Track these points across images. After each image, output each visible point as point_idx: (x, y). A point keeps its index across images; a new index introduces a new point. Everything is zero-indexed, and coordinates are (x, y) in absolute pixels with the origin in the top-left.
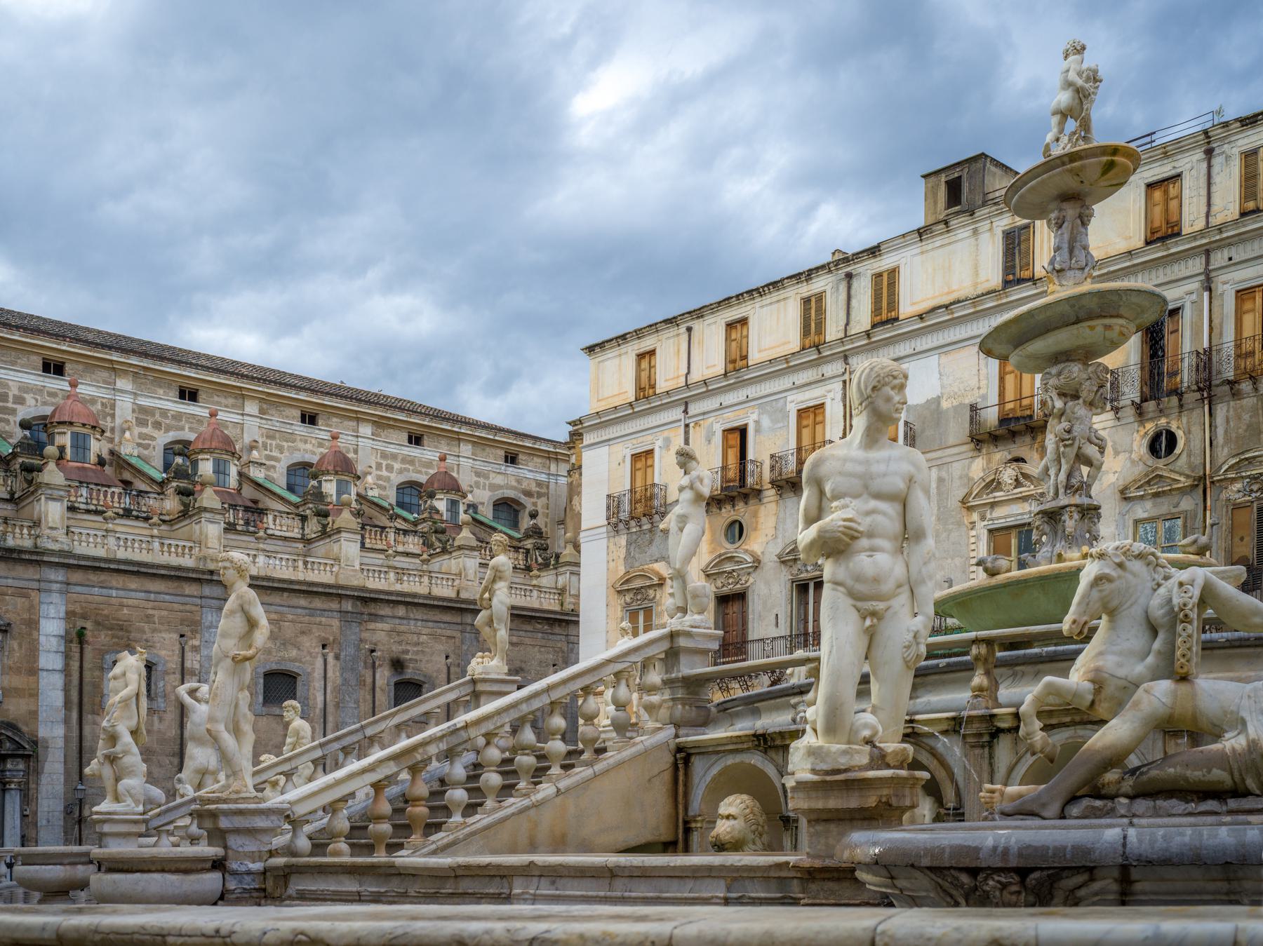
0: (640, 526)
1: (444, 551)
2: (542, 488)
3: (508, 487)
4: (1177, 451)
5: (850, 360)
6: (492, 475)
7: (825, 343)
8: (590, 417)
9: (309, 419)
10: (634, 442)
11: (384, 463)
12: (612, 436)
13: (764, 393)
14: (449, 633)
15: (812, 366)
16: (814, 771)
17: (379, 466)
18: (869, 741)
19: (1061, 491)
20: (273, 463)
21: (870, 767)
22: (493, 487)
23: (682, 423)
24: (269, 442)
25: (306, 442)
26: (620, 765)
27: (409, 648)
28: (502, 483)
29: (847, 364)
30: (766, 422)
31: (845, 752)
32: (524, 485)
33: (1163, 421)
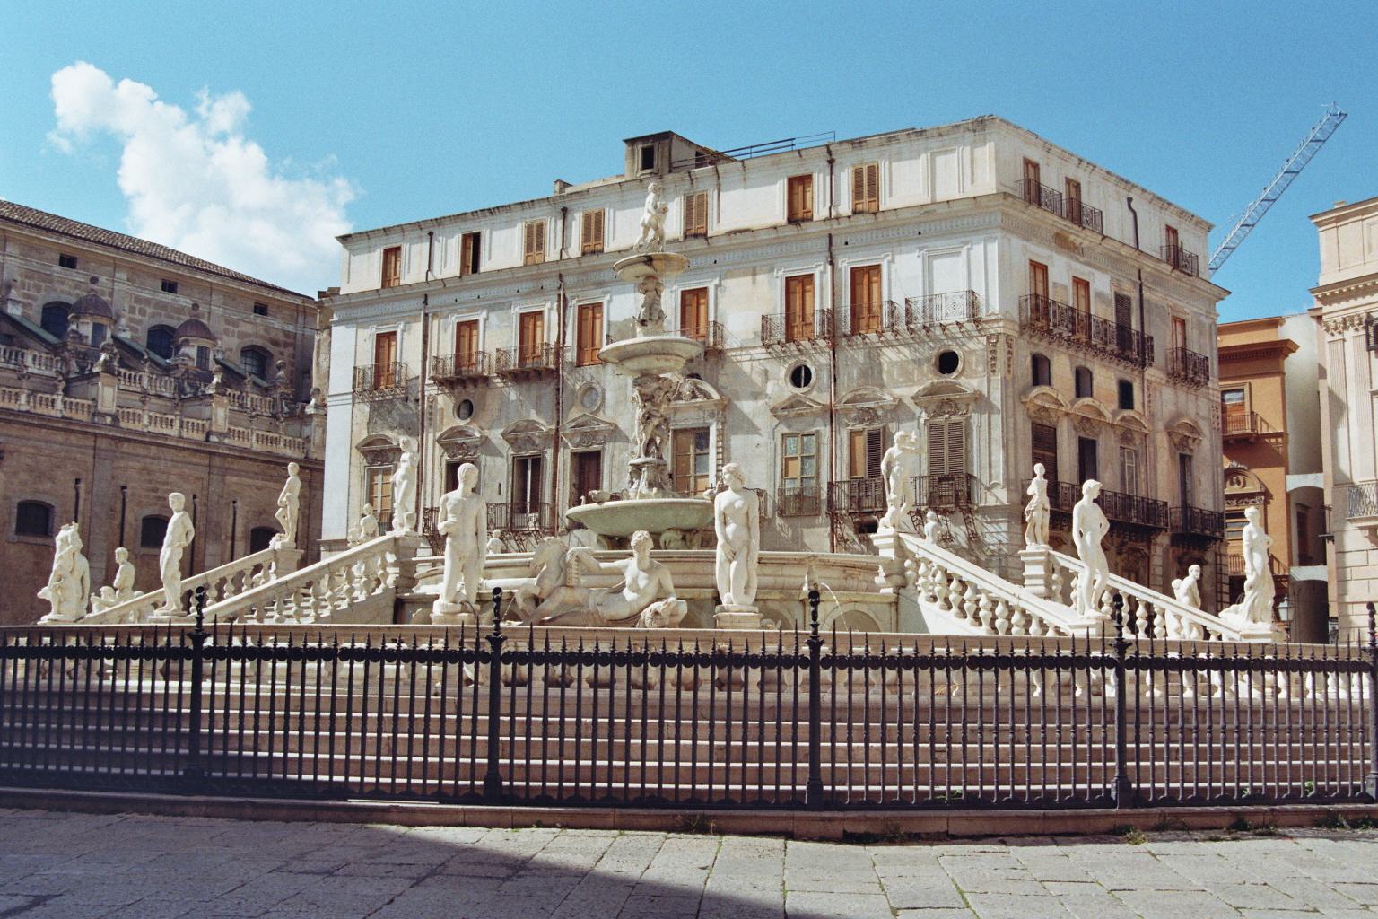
1: (195, 397)
3: (256, 336)
9: (68, 262)
11: (137, 306)
14: (197, 474)
17: (132, 310)
20: (29, 301)
22: (242, 335)
24: (27, 281)
25: (63, 283)
27: (158, 486)
28: (251, 332)
32: (273, 335)
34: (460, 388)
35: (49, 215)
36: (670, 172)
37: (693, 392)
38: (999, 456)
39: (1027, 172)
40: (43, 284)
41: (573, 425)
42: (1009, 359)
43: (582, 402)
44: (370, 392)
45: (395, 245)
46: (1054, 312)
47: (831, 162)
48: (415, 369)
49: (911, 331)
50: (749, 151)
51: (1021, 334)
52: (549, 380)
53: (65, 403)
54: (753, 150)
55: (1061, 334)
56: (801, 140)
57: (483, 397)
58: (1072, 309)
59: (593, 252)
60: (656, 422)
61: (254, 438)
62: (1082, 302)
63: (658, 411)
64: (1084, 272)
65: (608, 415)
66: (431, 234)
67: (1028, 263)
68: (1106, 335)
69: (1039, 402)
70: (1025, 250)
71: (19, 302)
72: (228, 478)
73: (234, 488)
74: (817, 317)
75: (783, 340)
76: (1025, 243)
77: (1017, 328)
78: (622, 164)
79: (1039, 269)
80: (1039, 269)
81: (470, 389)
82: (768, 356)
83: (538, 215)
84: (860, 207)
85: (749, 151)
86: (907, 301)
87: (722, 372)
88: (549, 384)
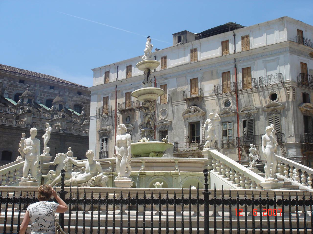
11: (43, 94)
17: (41, 95)
20: (11, 93)
22: (74, 101)
23: (115, 90)
24: (10, 87)
25: (20, 88)
32: (83, 100)
35: (18, 69)
36: (186, 43)
37: (194, 110)
38: (292, 127)
39: (298, 34)
40: (15, 88)
41: (159, 122)
42: (294, 95)
47: (234, 35)
51: (298, 86)
53: (16, 122)
57: (133, 115)
60: (149, 116)
61: (74, 130)
63: (150, 113)
65: (169, 119)
67: (300, 63)
69: (305, 108)
70: (298, 60)
71: (7, 94)
76: (299, 57)
77: (297, 85)
78: (172, 42)
82: (217, 98)
86: (259, 78)
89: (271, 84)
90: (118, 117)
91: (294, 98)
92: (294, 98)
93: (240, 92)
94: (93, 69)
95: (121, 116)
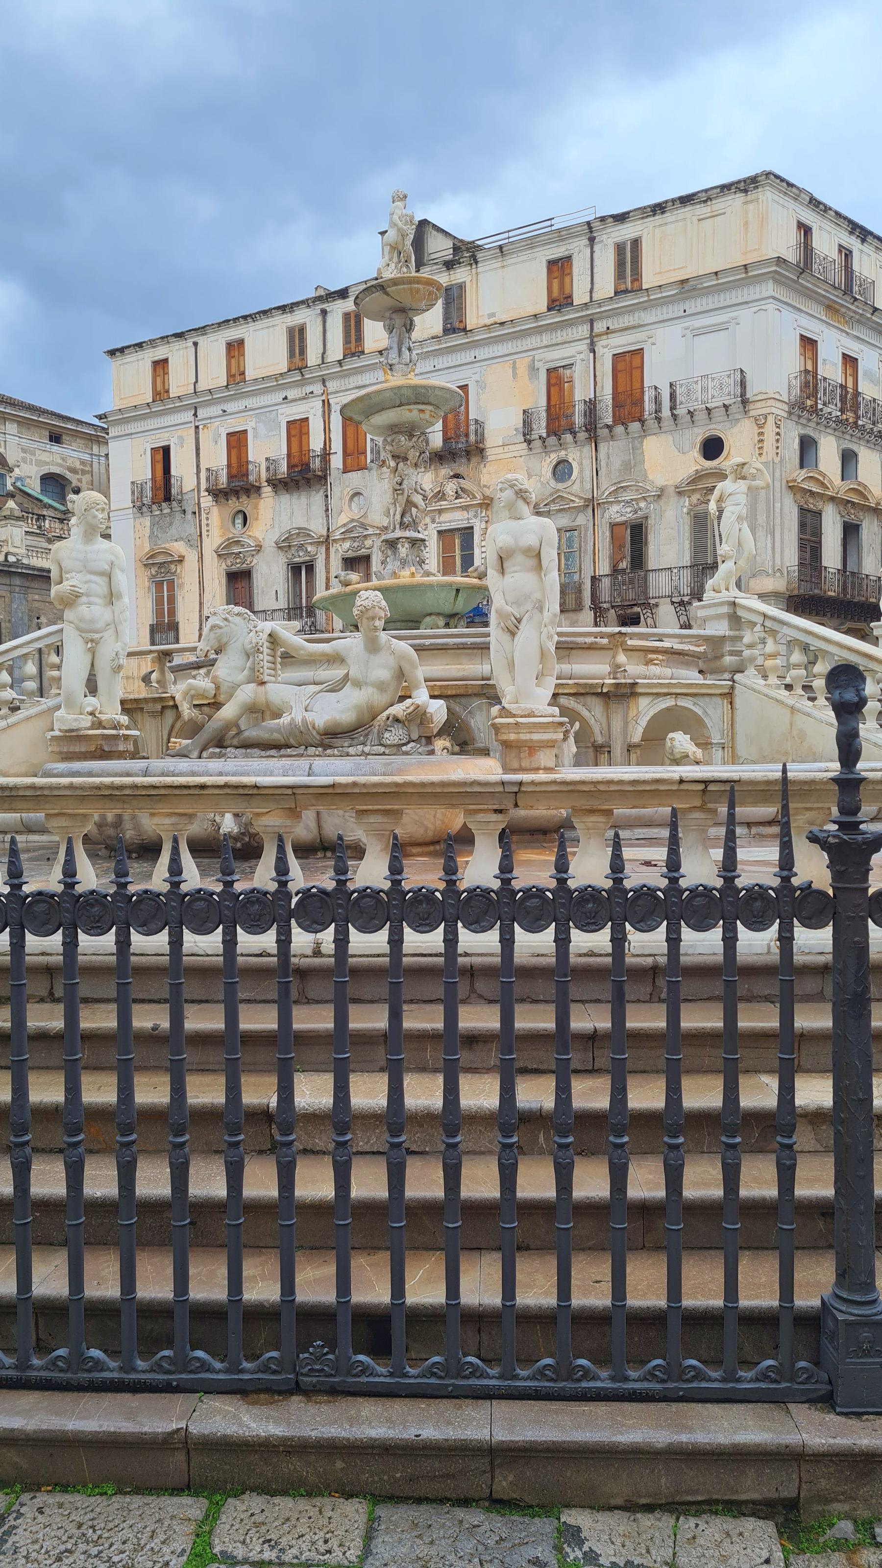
0: (161, 510)
2: (85, 466)
4: (573, 477)
5: (327, 384)
6: (37, 452)
7: (306, 367)
8: (113, 412)
10: (153, 437)
12: (133, 431)
13: (259, 405)
15: (298, 386)
16: (60, 730)
18: (92, 714)
19: (398, 526)
21: (91, 728)
22: (40, 463)
23: (193, 425)
26: (28, 719)
28: (48, 460)
29: (325, 386)
30: (262, 430)
31: (76, 720)
32: (69, 463)
33: (563, 453)
34: (234, 499)
37: (456, 493)
41: (343, 530)
42: (778, 441)
43: (350, 506)
44: (150, 507)
45: (161, 357)
46: (825, 390)
47: (592, 240)
48: (189, 483)
49: (675, 417)
50: (506, 235)
51: (790, 413)
52: (319, 486)
54: (511, 234)
55: (830, 413)
56: (562, 219)
57: (256, 507)
58: (841, 385)
59: (353, 355)
62: (850, 380)
64: (854, 348)
66: (195, 344)
68: (874, 415)
72: (30, 597)
73: (37, 605)
74: (579, 408)
75: (544, 435)
77: (786, 408)
79: (808, 344)
80: (808, 344)
81: (244, 498)
83: (300, 316)
84: (623, 287)
85: (506, 235)
86: (671, 385)
87: (485, 471)
88: (318, 491)
89: (708, 405)
90: (208, 514)
91: (777, 454)
92: (777, 454)
93: (603, 433)
94: (108, 352)
95: (215, 511)
